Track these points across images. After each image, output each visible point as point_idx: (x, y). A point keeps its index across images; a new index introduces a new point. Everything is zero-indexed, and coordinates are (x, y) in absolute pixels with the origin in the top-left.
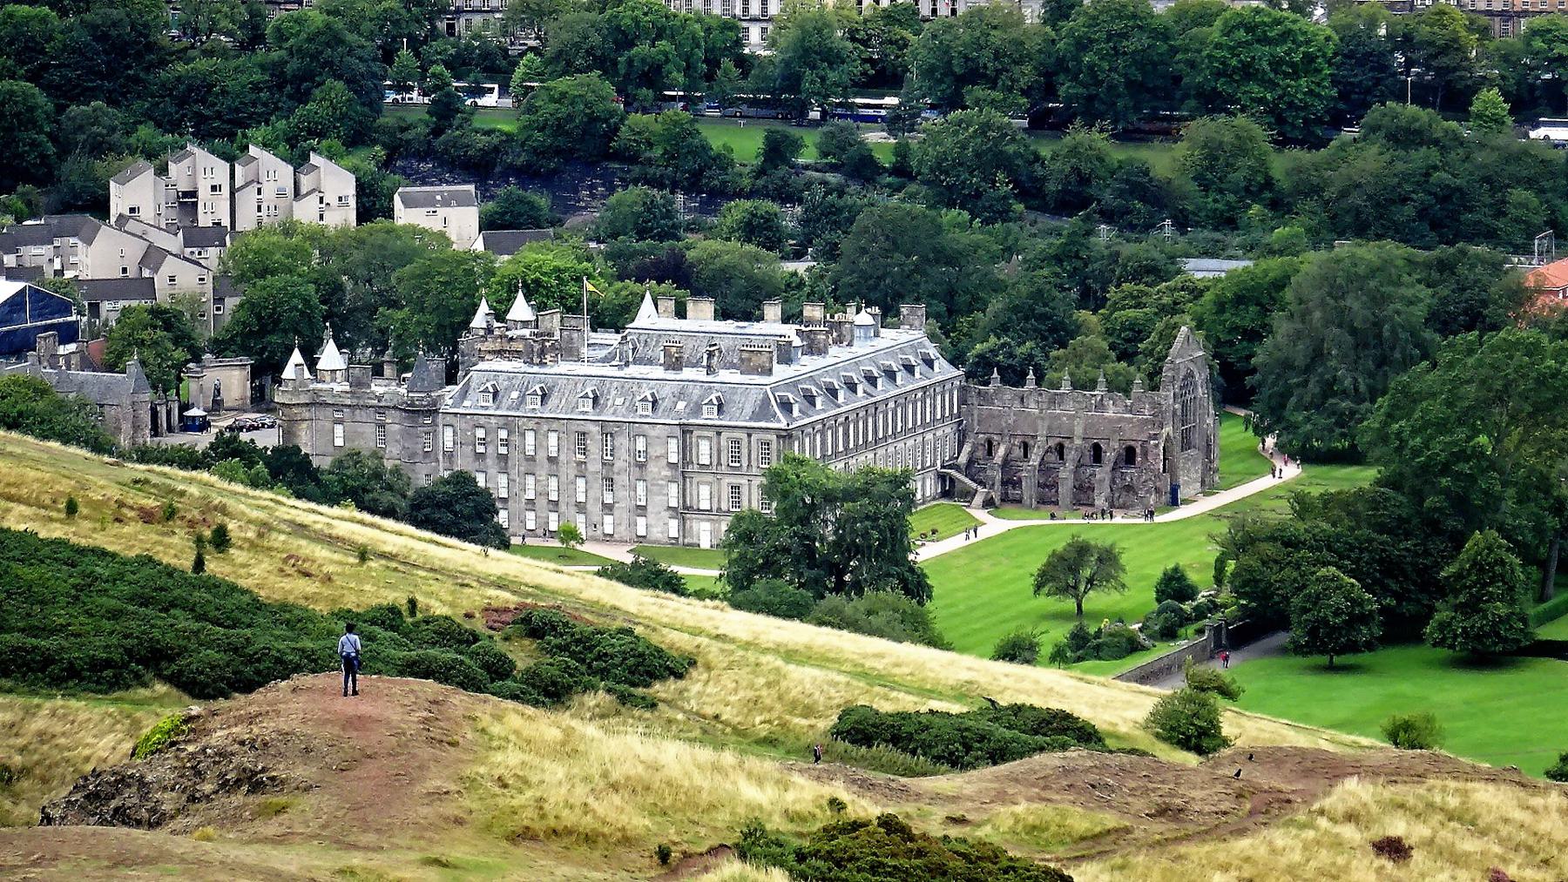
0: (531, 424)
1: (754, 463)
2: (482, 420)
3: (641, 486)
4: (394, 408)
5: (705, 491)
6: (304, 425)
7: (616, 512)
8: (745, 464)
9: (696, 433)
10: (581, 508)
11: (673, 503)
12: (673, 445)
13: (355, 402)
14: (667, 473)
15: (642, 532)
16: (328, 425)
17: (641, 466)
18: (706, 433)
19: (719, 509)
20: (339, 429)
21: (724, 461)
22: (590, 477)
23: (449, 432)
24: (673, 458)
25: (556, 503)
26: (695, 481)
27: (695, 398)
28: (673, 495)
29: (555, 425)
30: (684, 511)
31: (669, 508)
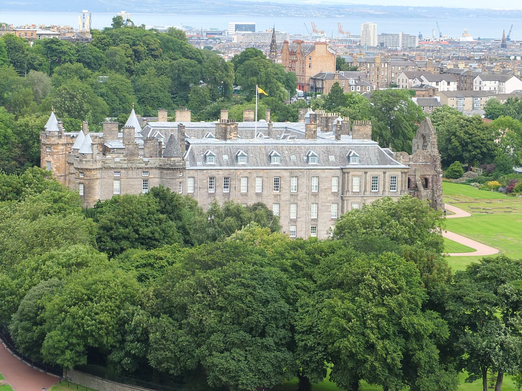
0: (246, 174)
1: (387, 189)
3: (314, 208)
6: (98, 182)
7: (298, 224)
8: (381, 190)
12: (335, 181)
13: (130, 165)
14: (331, 198)
17: (315, 195)
18: (358, 173)
22: (282, 204)
23: (190, 182)
24: (335, 189)
26: (350, 202)
27: (338, 154)
29: (261, 174)
31: (332, 219)
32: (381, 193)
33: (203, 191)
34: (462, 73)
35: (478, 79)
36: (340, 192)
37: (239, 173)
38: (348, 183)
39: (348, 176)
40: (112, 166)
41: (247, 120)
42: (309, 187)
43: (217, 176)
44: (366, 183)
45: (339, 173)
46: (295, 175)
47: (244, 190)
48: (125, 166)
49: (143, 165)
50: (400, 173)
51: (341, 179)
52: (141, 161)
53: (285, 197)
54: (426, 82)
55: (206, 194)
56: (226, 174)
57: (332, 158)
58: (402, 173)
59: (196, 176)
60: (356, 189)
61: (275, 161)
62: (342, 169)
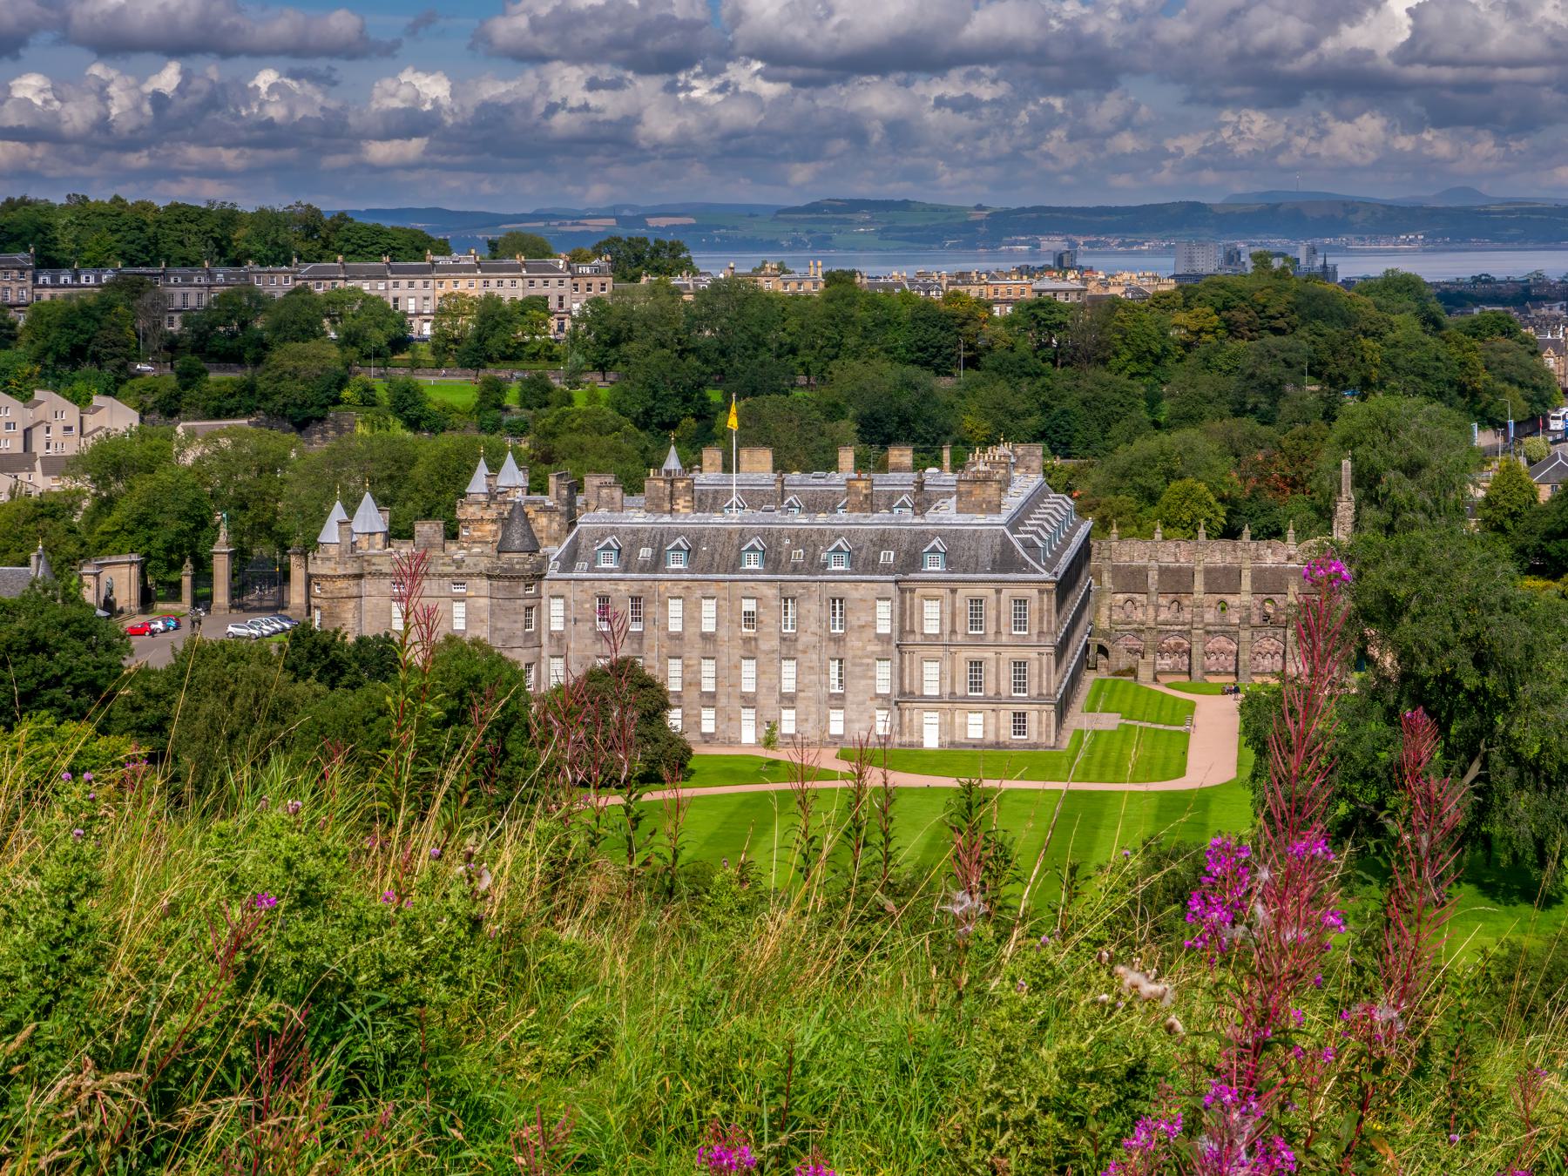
4: (480, 575)
5: (931, 671)
7: (800, 704)
8: (992, 629)
10: (749, 701)
11: (883, 688)
12: (884, 610)
15: (836, 728)
16: (384, 602)
17: (837, 640)
18: (936, 592)
19: (953, 693)
21: (959, 627)
22: (762, 657)
23: (557, 607)
24: (884, 628)
25: (713, 696)
28: (883, 678)
29: (712, 589)
30: (904, 698)
31: (878, 696)
32: (991, 638)
33: (585, 627)
36: (896, 635)
37: (662, 589)
38: (912, 614)
39: (912, 599)
41: (897, 469)
43: (613, 595)
44: (953, 615)
45: (892, 589)
46: (790, 593)
47: (675, 626)
49: (452, 569)
50: (1035, 592)
51: (897, 604)
52: (447, 560)
53: (769, 644)
55: (591, 634)
56: (635, 588)
58: (1041, 592)
59: (569, 595)
62: (896, 582)
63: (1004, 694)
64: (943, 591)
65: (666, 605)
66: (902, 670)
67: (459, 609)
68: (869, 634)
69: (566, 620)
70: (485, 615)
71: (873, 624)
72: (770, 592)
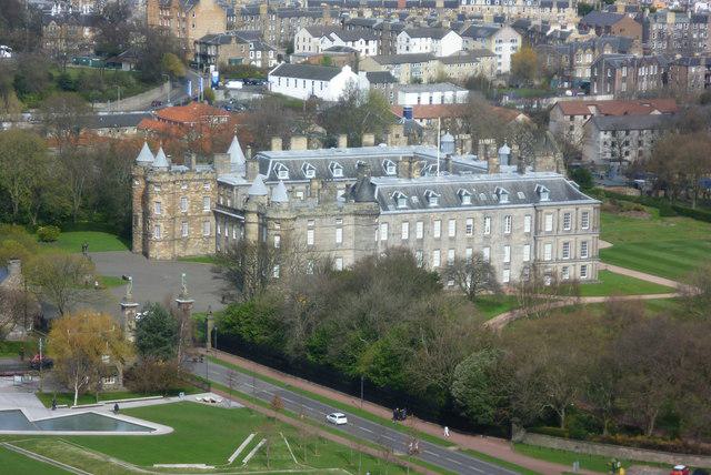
2: (408, 217)
9: (545, 211)
12: (527, 219)
17: (508, 236)
20: (311, 234)
23: (384, 228)
24: (527, 230)
29: (455, 215)
34: (374, 26)
35: (403, 35)
40: (306, 214)
42: (503, 229)
45: (532, 211)
47: (437, 235)
48: (320, 214)
49: (336, 212)
54: (339, 42)
57: (521, 195)
60: (549, 228)
61: (467, 201)
63: (578, 256)
64: (553, 210)
65: (433, 224)
66: (535, 248)
67: (339, 231)
68: (521, 233)
69: (389, 235)
70: (352, 234)
71: (522, 228)
72: (479, 215)
